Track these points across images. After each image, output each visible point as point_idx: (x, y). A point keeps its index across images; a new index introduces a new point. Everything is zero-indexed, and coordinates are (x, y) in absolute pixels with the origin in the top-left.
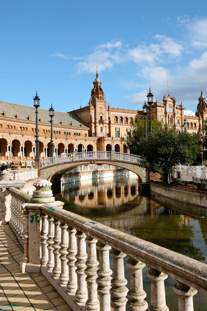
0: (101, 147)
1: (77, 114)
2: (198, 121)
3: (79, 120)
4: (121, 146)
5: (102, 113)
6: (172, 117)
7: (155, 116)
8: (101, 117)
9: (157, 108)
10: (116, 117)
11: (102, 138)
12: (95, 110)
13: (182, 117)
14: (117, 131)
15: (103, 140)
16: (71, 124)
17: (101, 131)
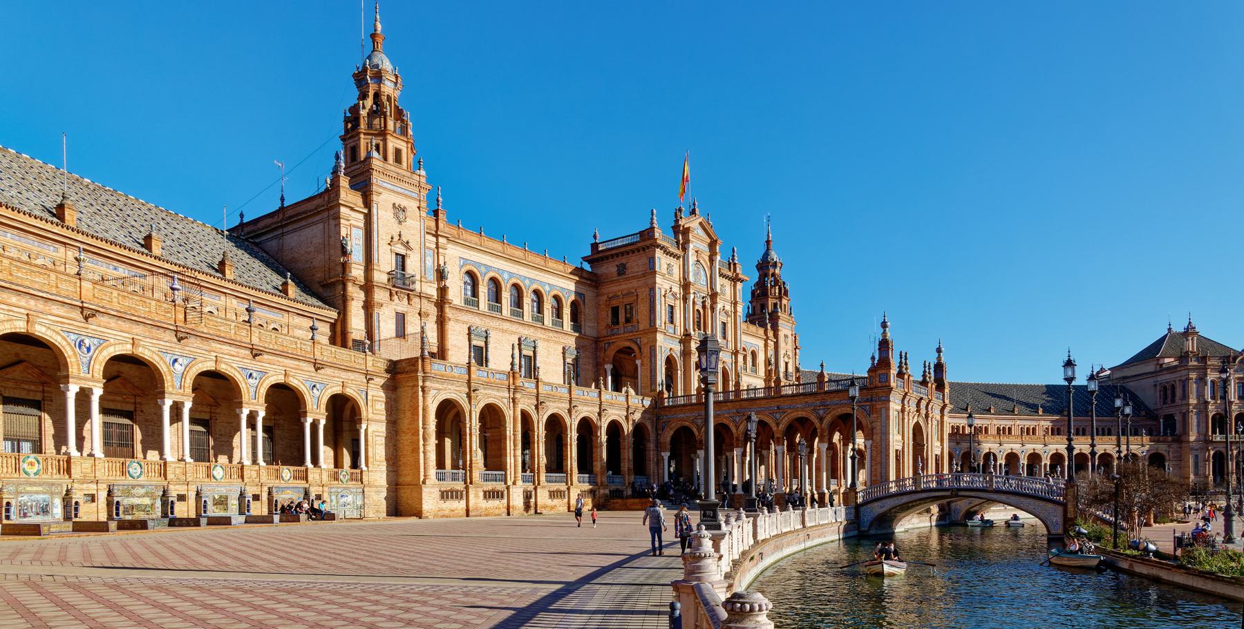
0: (408, 414)
1: (264, 238)
2: (761, 344)
3: (277, 263)
4: (509, 414)
5: (405, 240)
6: (704, 307)
7: (643, 293)
8: (402, 260)
9: (652, 260)
10: (470, 274)
11: (412, 362)
12: (368, 218)
13: (735, 312)
14: (474, 343)
15: (420, 374)
16: (222, 263)
17: (394, 326)
